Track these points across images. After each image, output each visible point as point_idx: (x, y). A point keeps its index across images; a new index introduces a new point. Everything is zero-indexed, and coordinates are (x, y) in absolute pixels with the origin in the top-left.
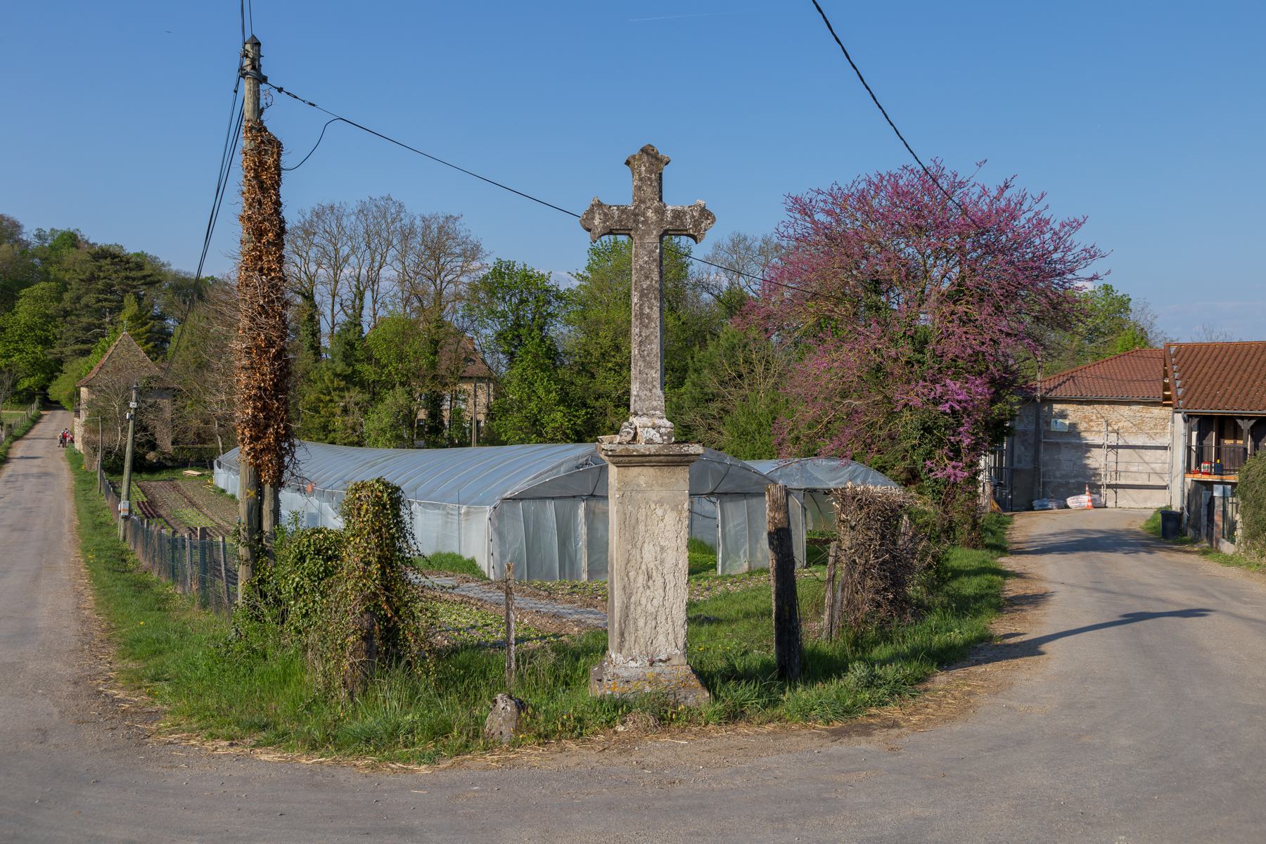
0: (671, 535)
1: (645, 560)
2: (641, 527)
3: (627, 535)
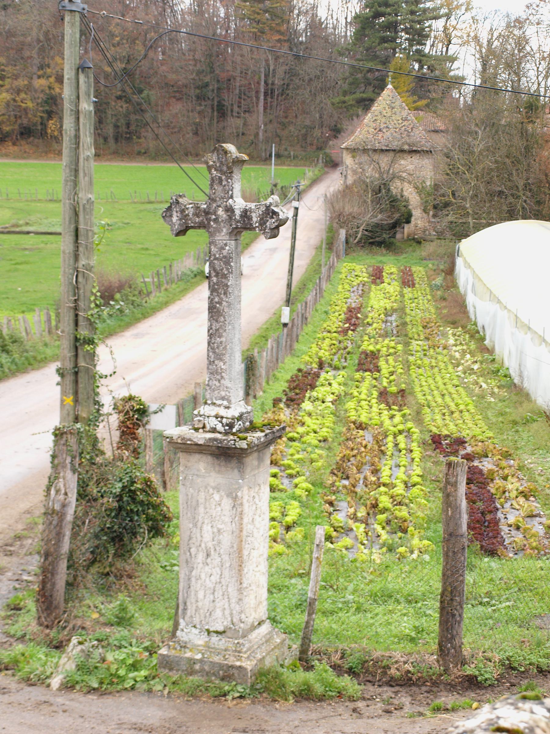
0: (227, 519)
1: (204, 540)
2: (201, 509)
3: (189, 515)
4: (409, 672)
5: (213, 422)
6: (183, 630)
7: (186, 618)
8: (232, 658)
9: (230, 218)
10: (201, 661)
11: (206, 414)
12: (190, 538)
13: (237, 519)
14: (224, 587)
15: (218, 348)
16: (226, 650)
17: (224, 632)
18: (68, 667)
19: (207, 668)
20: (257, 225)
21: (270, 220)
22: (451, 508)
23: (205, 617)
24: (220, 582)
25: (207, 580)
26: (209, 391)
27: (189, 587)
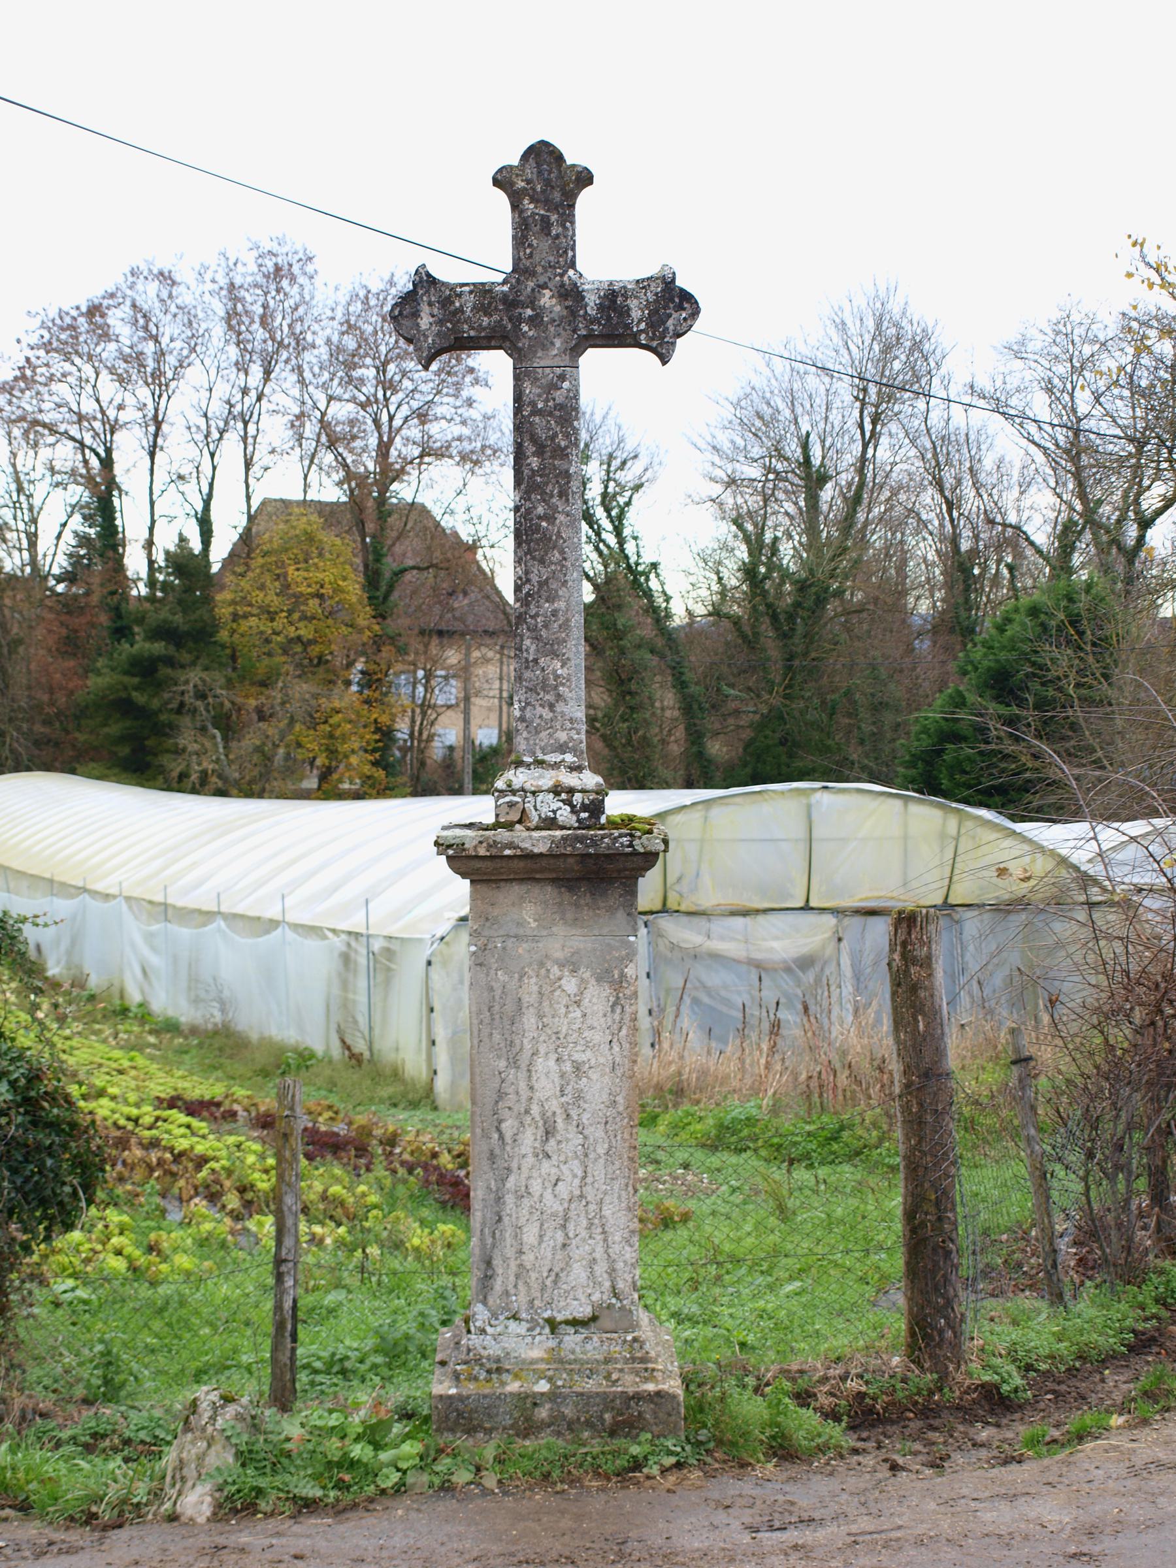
0: (598, 1037)
1: (538, 1095)
2: (529, 1021)
3: (497, 1037)
4: (861, 1396)
5: (548, 804)
6: (483, 1331)
7: (491, 1301)
8: (629, 1378)
9: (573, 313)
10: (553, 1396)
11: (528, 786)
12: (501, 1095)
13: (624, 1032)
14: (592, 1207)
15: (546, 626)
16: (607, 1361)
17: (594, 1318)
18: (212, 1460)
19: (568, 1411)
20: (643, 326)
21: (675, 315)
22: (925, 1016)
23: (543, 1288)
24: (582, 1196)
25: (548, 1195)
26: (525, 734)
27: (500, 1220)
